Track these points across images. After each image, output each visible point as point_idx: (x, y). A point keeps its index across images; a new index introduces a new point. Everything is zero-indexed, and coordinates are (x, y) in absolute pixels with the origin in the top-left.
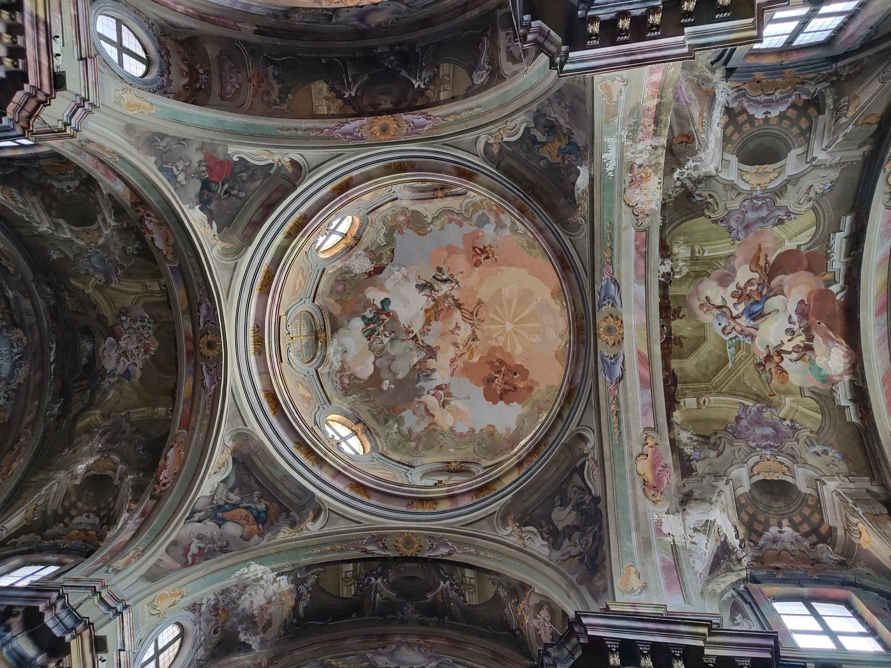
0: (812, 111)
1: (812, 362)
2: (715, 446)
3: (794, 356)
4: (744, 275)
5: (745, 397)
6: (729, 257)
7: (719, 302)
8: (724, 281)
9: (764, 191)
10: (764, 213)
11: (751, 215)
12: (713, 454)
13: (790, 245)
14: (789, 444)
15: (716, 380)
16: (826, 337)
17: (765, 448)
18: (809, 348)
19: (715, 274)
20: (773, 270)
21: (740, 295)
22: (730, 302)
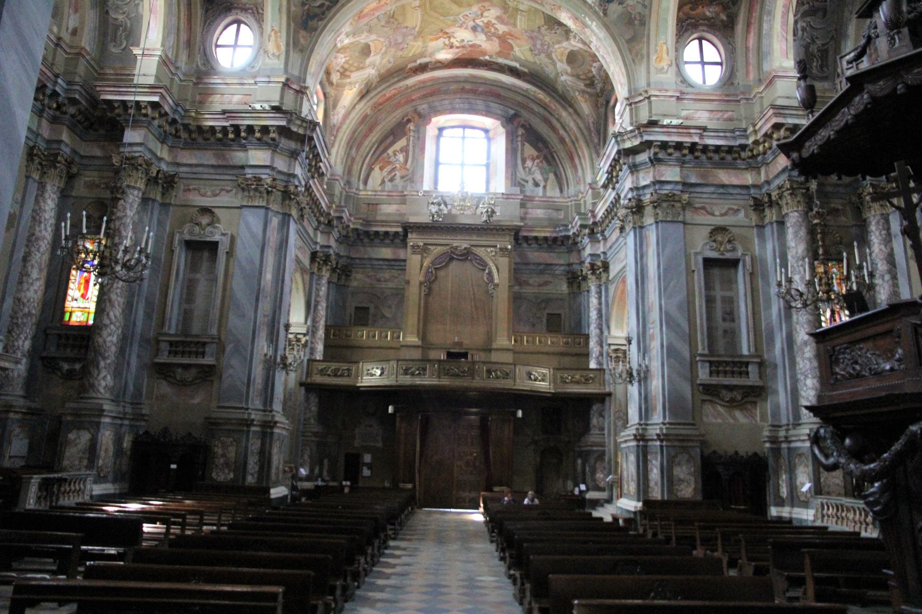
0: (588, 82)
1: (443, 49)
2: (388, 22)
3: (447, 42)
4: (502, 29)
5: (421, 27)
6: (515, 25)
7: (485, 14)
8: (498, 18)
9: (551, 52)
10: (538, 46)
11: (539, 43)
12: (383, 23)
13: (516, 49)
14: (393, 50)
15: (432, 13)
16: (457, 53)
17: (390, 42)
18: (452, 47)
19: (505, 17)
20: (503, 39)
21: (488, 24)
22: (485, 20)
